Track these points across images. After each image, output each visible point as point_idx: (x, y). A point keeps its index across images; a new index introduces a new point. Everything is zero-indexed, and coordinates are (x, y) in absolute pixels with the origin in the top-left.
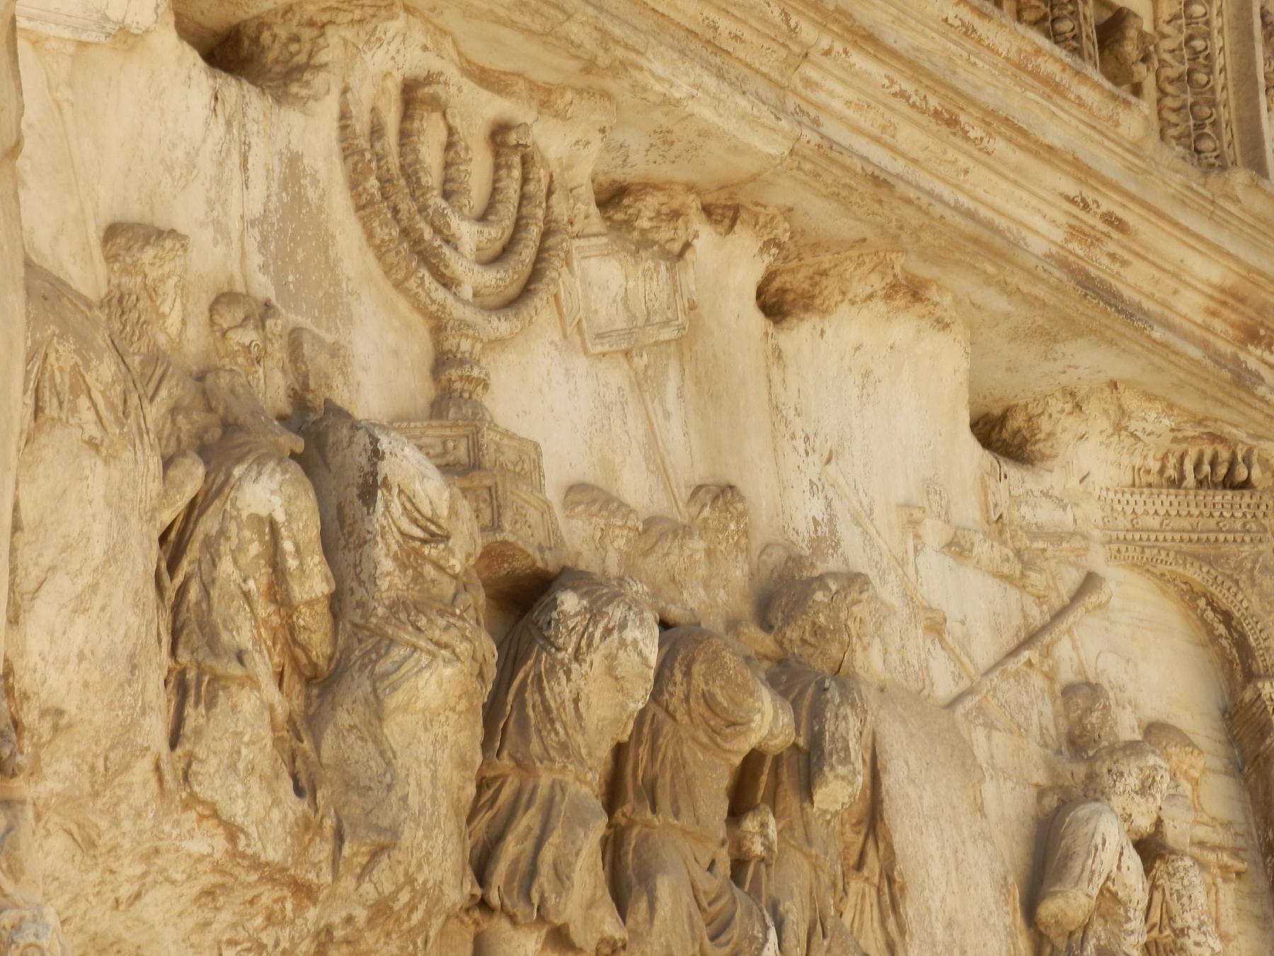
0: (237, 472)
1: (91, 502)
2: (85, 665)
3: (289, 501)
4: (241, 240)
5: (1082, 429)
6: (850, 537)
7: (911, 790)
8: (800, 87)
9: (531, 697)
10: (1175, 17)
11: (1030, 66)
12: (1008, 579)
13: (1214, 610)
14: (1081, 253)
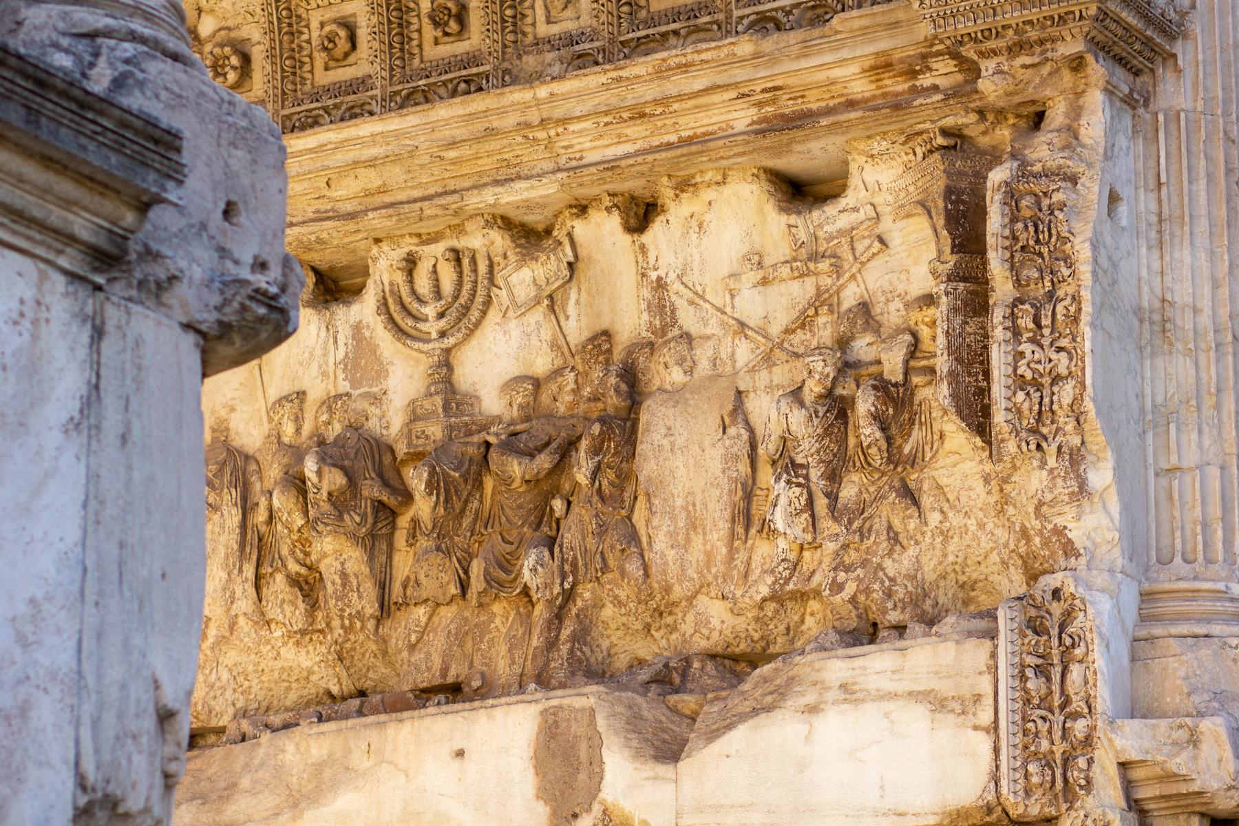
7: (665, 442)
8: (563, 151)
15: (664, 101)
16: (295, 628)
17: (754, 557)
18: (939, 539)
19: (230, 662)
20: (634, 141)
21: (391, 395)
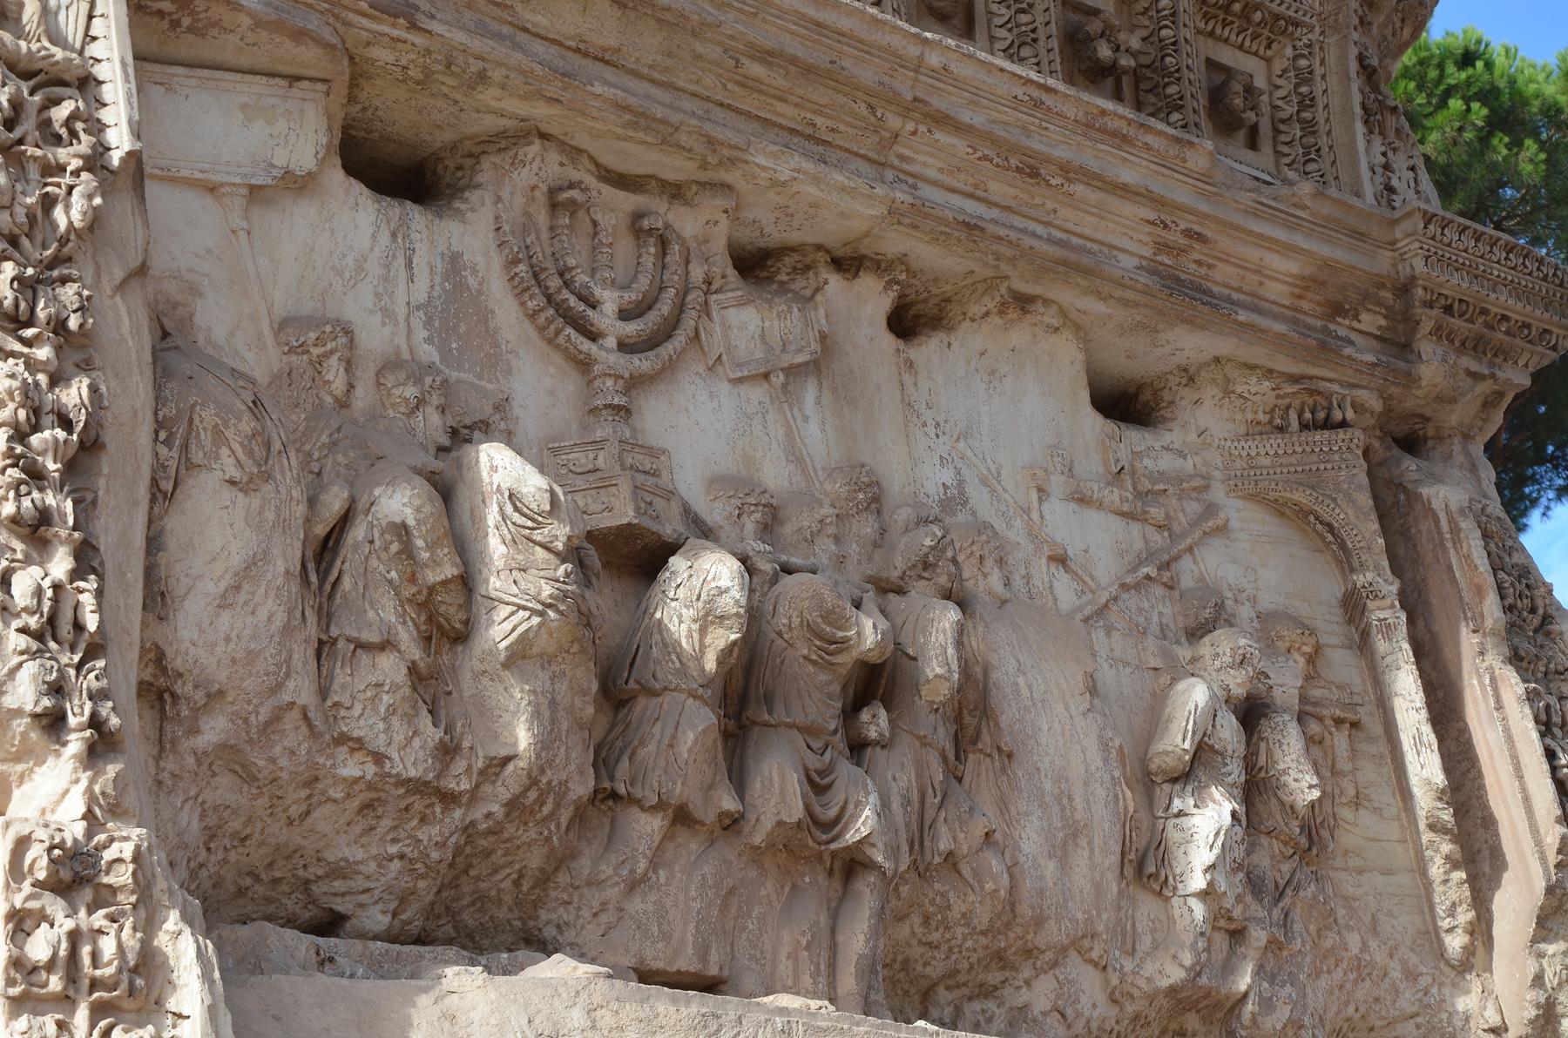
0: (377, 492)
1: (231, 525)
2: (232, 646)
3: (418, 510)
4: (407, 320)
5: (1196, 396)
6: (979, 497)
9: (656, 637)
10: (1285, 71)
11: (1097, 125)
12: (1128, 516)
13: (1321, 523)
14: (1170, 263)
15: (1067, 170)
16: (412, 773)
17: (1138, 915)
18: (1352, 976)
19: (210, 797)
20: (990, 204)
21: (517, 411)
